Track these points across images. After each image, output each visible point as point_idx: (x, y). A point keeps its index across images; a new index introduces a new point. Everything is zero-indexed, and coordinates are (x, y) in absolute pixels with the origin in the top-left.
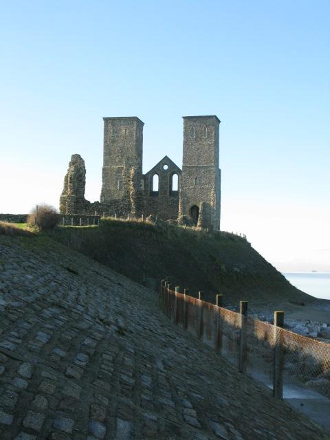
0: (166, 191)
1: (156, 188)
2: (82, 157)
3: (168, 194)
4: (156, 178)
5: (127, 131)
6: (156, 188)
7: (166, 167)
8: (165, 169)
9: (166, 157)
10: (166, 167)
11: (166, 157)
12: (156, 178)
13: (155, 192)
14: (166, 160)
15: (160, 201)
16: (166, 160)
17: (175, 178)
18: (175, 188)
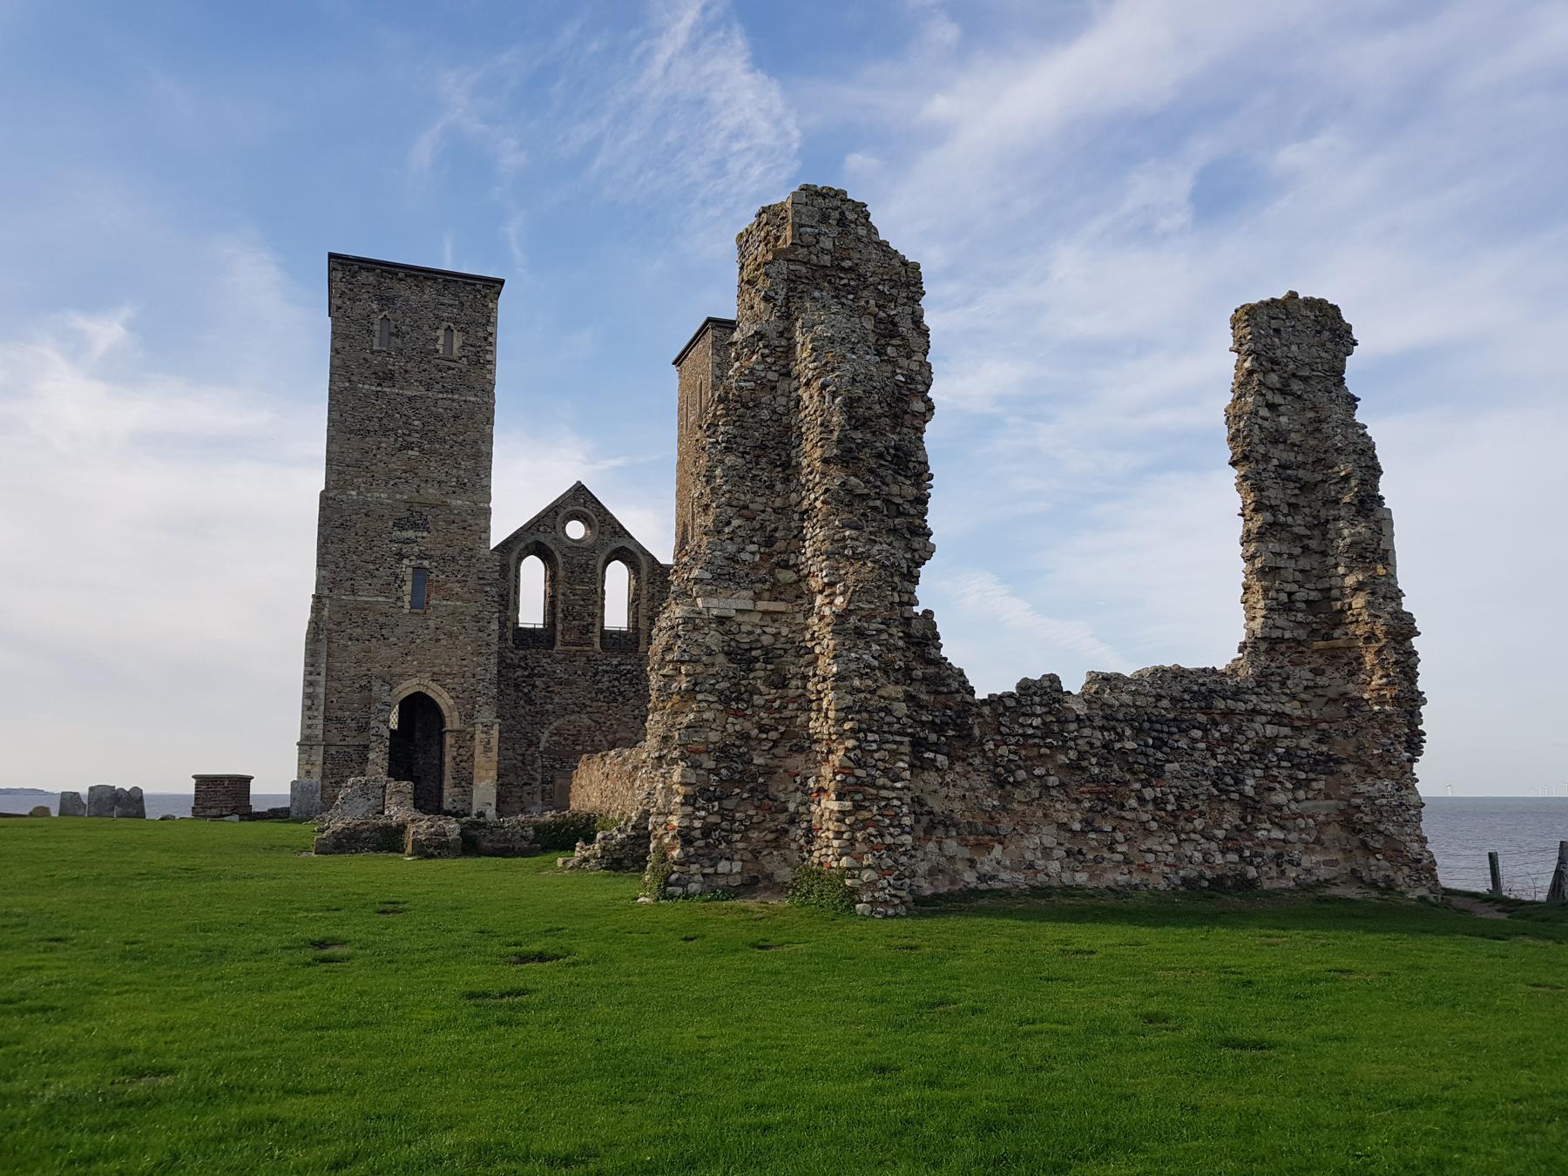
0: (586, 630)
1: (531, 613)
2: (893, 246)
3: (597, 640)
4: (533, 573)
5: (457, 343)
6: (531, 613)
7: (576, 530)
8: (578, 535)
9: (579, 491)
10: (576, 530)
11: (579, 491)
12: (533, 573)
13: (532, 631)
14: (579, 501)
15: (559, 669)
16: (579, 501)
17: (617, 578)
18: (616, 616)
